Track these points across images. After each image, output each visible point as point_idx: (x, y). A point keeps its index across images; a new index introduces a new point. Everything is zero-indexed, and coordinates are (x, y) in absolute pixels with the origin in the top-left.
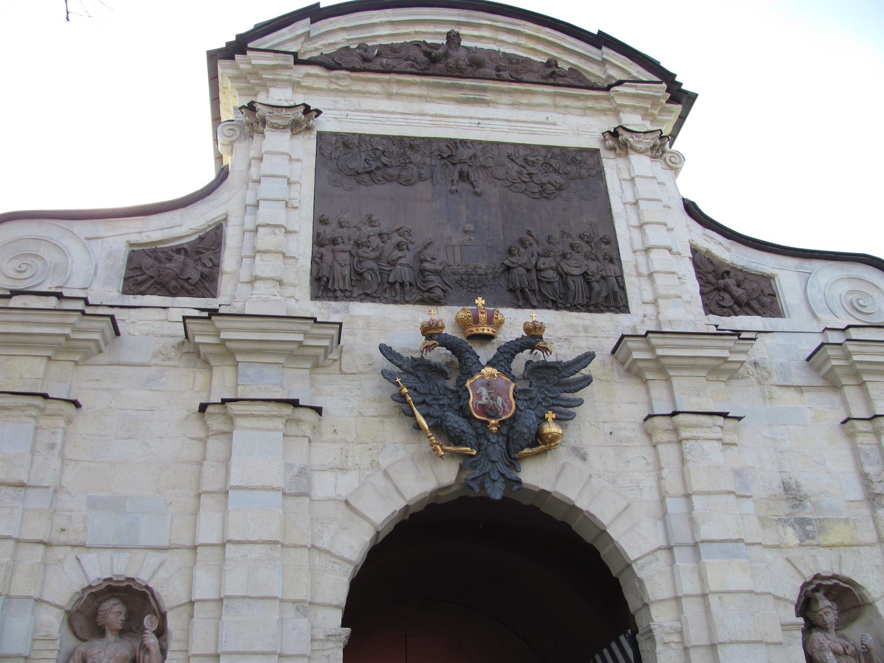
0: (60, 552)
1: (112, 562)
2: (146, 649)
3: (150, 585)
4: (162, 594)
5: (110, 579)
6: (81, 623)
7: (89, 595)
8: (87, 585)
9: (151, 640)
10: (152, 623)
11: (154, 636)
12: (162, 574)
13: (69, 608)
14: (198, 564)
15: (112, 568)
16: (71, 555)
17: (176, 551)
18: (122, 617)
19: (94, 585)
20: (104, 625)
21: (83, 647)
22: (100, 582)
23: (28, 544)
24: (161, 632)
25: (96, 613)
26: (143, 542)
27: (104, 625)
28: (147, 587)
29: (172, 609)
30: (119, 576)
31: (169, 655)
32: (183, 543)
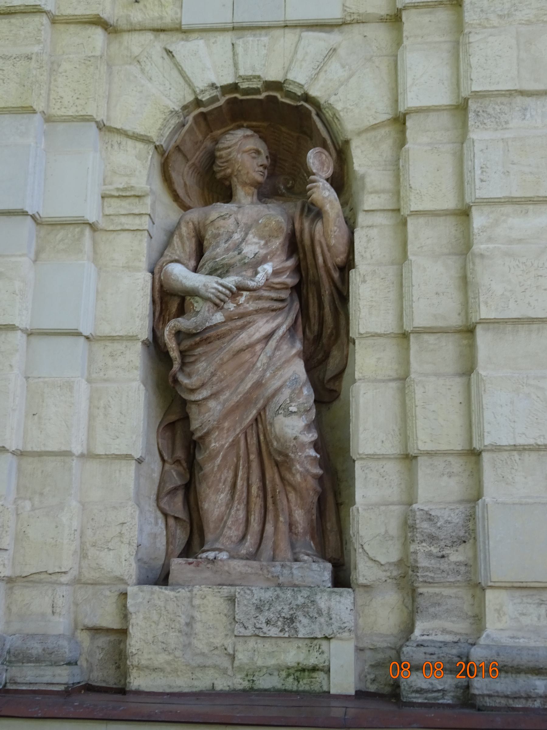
0: (135, 43)
1: (235, 54)
2: (315, 212)
3: (314, 92)
4: (339, 106)
5: (234, 87)
6: (184, 176)
7: (195, 118)
8: (190, 98)
9: (324, 193)
10: (322, 164)
11: (328, 185)
12: (335, 70)
13: (162, 142)
14: (406, 42)
15: (236, 65)
16: (155, 46)
17: (356, 28)
18: (263, 160)
19: (205, 97)
20: (228, 178)
21: (194, 215)
22: (215, 93)
23: (72, 28)
24: (340, 181)
25: (212, 158)
26: (295, 14)
27: (228, 178)
28: (307, 98)
29: (359, 133)
30: (248, 79)
31: (362, 219)
32: (370, 10)
